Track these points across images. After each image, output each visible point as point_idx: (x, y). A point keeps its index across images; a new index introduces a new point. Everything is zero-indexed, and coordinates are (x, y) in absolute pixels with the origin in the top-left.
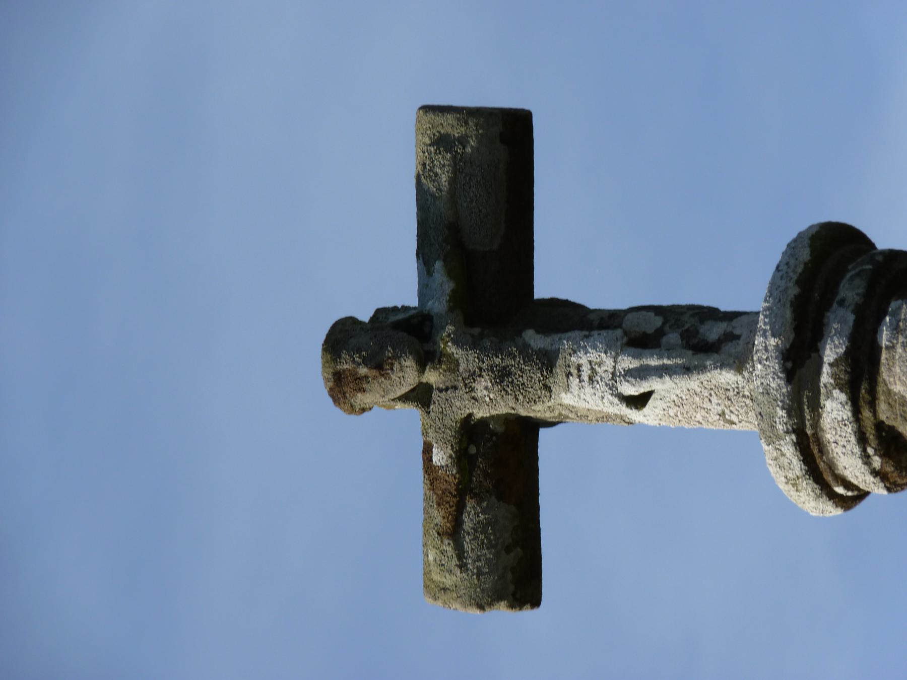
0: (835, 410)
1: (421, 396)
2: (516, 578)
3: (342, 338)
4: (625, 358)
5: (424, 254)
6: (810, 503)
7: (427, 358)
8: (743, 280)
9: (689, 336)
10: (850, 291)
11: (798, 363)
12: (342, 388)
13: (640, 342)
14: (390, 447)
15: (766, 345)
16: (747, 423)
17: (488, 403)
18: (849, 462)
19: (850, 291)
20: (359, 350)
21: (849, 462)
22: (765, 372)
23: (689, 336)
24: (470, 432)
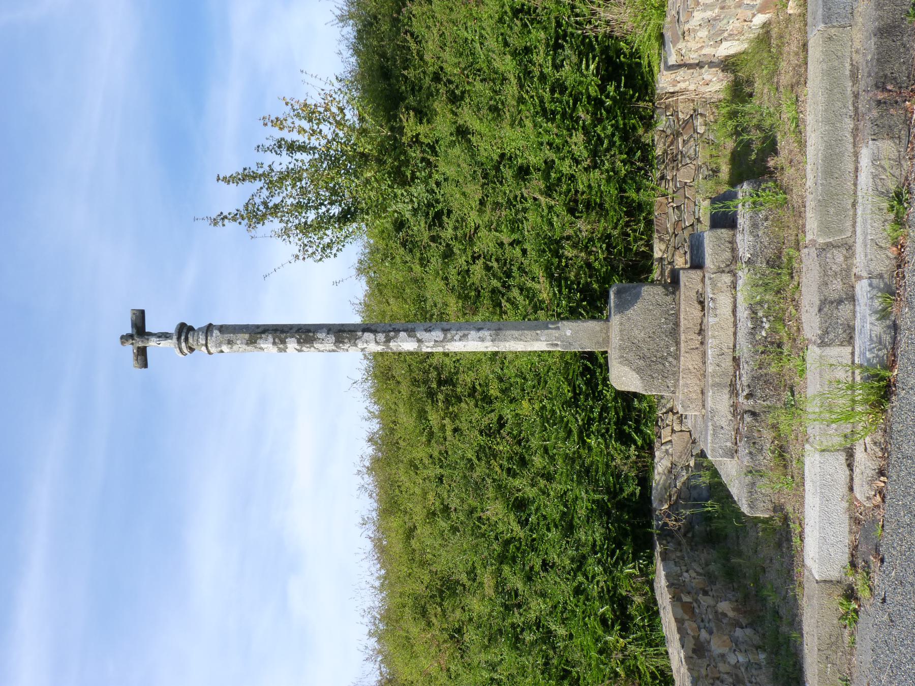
0: (183, 345)
1: (132, 344)
2: (145, 365)
3: (122, 337)
4: (725, 83)
5: (132, 327)
6: (180, 355)
7: (133, 339)
8: (172, 329)
9: (165, 336)
10: (185, 330)
11: (179, 339)
12: (122, 343)
13: (159, 337)
14: (129, 350)
15: (175, 337)
16: (172, 346)
17: (141, 345)
18: (185, 350)
19: (185, 330)
20: (125, 338)
21: (185, 350)
22: (175, 340)
23: (165, 336)
24: (139, 348)
